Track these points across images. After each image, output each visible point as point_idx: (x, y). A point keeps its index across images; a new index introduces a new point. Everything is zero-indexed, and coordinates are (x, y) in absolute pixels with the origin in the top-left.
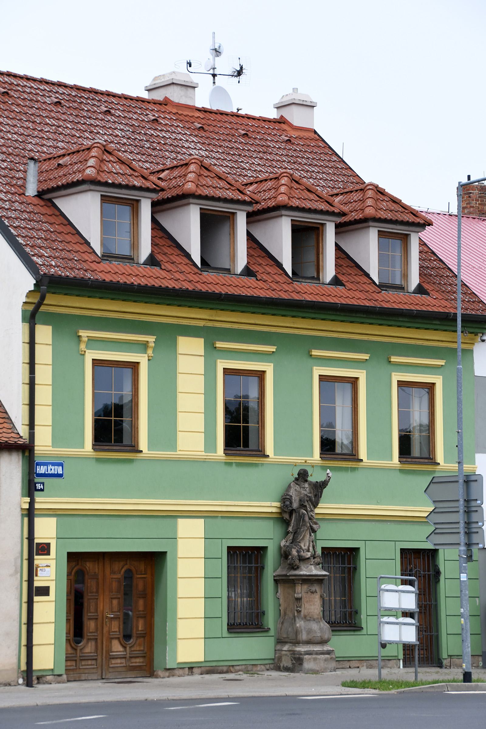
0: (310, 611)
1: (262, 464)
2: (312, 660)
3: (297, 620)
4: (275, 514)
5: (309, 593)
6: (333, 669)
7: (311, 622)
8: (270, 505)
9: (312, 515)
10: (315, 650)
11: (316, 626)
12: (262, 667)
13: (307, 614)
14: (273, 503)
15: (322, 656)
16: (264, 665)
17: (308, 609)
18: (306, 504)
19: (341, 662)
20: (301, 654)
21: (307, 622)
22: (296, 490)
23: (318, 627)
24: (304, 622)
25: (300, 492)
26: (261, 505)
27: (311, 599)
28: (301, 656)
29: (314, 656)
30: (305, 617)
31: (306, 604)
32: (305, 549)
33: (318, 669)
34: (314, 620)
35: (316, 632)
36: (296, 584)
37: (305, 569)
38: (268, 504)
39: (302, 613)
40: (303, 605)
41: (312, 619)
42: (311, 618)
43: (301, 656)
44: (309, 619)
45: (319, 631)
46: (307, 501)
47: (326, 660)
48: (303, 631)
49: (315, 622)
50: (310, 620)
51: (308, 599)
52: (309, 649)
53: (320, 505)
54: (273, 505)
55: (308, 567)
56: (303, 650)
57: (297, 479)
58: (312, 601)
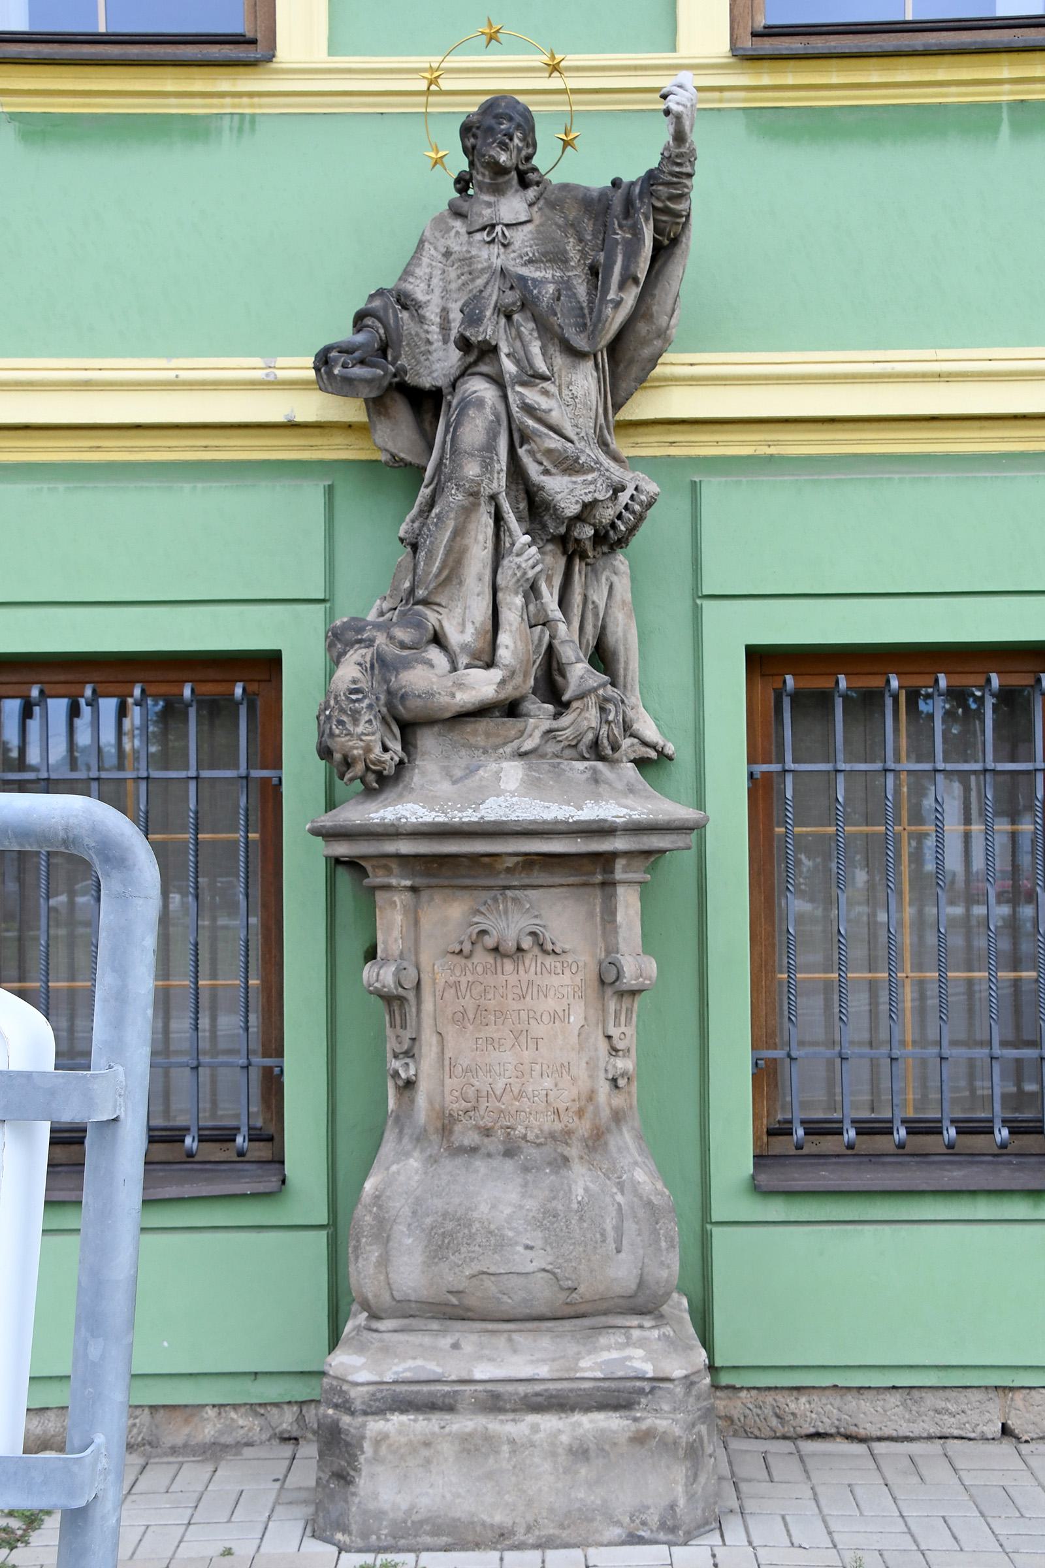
0: (481, 1082)
1: (246, 124)
2: (447, 1448)
3: (388, 1147)
4: (339, 439)
5: (482, 958)
6: (654, 1519)
7: (479, 1164)
8: (259, 375)
9: (529, 409)
10: (478, 1375)
11: (514, 1196)
12: (241, 1420)
13: (456, 1106)
14: (281, 361)
15: (549, 1422)
16: (254, 1408)
17: (467, 1070)
18: (491, 329)
19: (930, 1399)
20: (346, 1406)
21: (449, 1165)
22: (447, 254)
23: (530, 1204)
24: (433, 1160)
25: (467, 260)
26: (185, 375)
27: (492, 1004)
28: (346, 1419)
29: (465, 1423)
30: (446, 1124)
31: (450, 1032)
32: (464, 647)
33: (499, 1518)
34: (509, 1153)
35: (501, 1244)
36: (380, 896)
37: (445, 787)
38: (250, 367)
39: (422, 1099)
40: (429, 1039)
41: (494, 1144)
42: (487, 1132)
43: (346, 1419)
44: (470, 1138)
45: (535, 1237)
46: (509, 317)
47: (580, 1452)
48: (401, 1228)
49: (509, 1165)
50: (473, 1150)
51: (469, 1003)
52: (432, 1367)
53: (672, 363)
54: (282, 375)
55: (471, 771)
56: (363, 1376)
57: (463, 183)
58: (501, 1013)
